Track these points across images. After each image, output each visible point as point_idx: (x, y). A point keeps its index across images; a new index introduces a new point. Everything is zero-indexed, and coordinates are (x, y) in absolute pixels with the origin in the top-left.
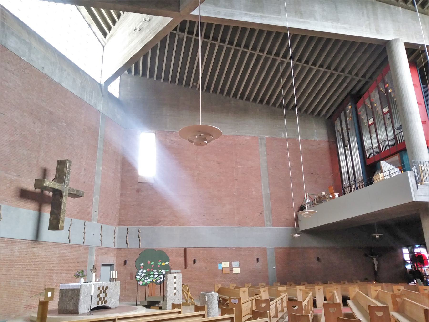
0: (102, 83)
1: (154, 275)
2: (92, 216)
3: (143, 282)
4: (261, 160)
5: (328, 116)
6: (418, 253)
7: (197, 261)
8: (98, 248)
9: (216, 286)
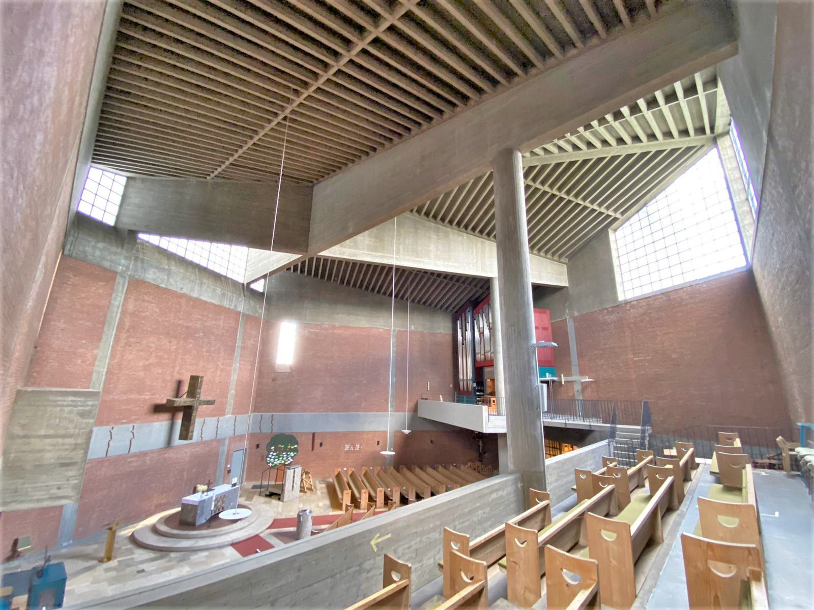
0: (245, 283)
1: (283, 457)
2: (227, 410)
3: (272, 463)
5: (455, 310)
7: (323, 444)
8: (230, 438)
9: (336, 470)
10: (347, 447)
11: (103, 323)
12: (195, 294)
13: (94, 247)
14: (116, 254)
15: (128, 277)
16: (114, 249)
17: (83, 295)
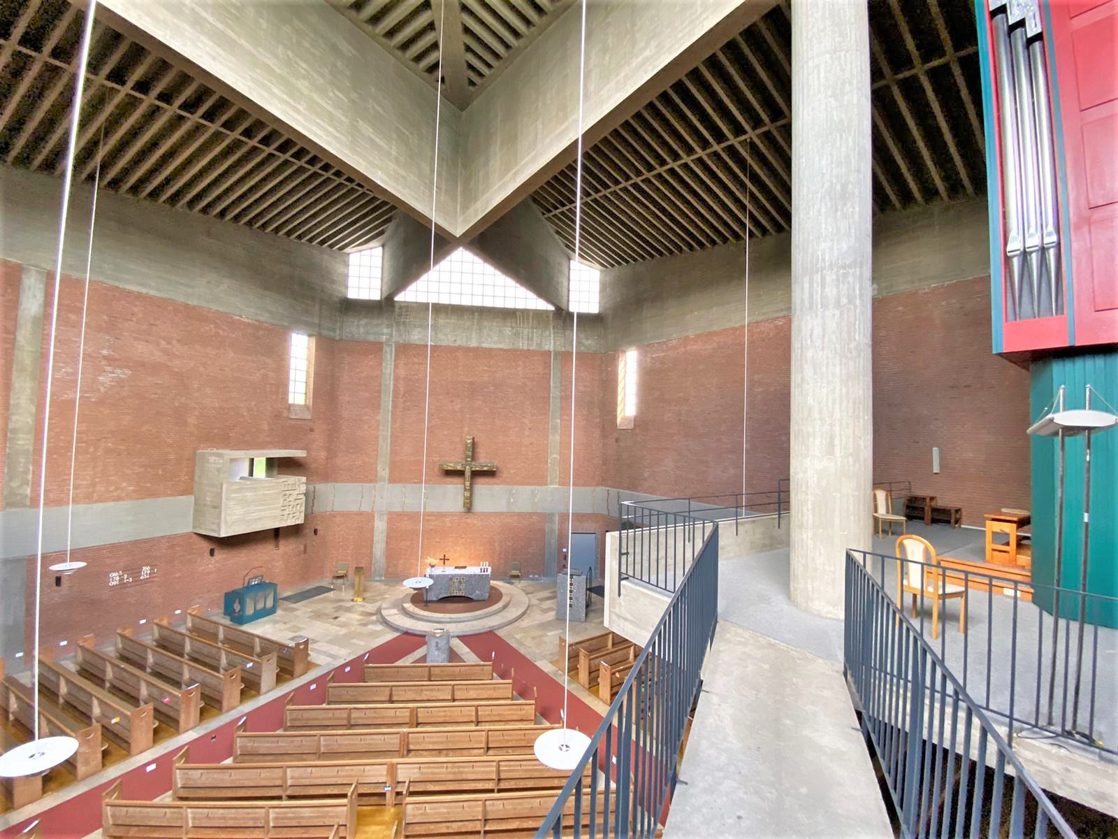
2: (549, 479)
11: (379, 392)
12: (474, 344)
13: (358, 326)
14: (377, 325)
15: (393, 344)
16: (376, 321)
17: (358, 370)
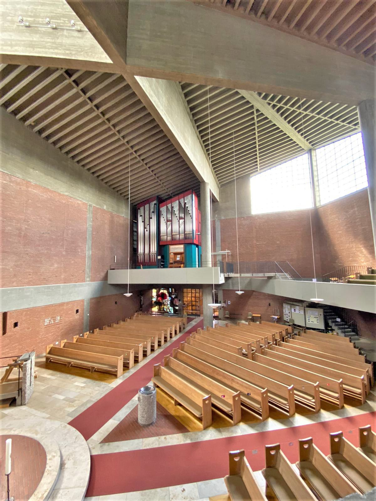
4: (88, 225)
6: (162, 293)
7: (19, 324)
10: (47, 321)
